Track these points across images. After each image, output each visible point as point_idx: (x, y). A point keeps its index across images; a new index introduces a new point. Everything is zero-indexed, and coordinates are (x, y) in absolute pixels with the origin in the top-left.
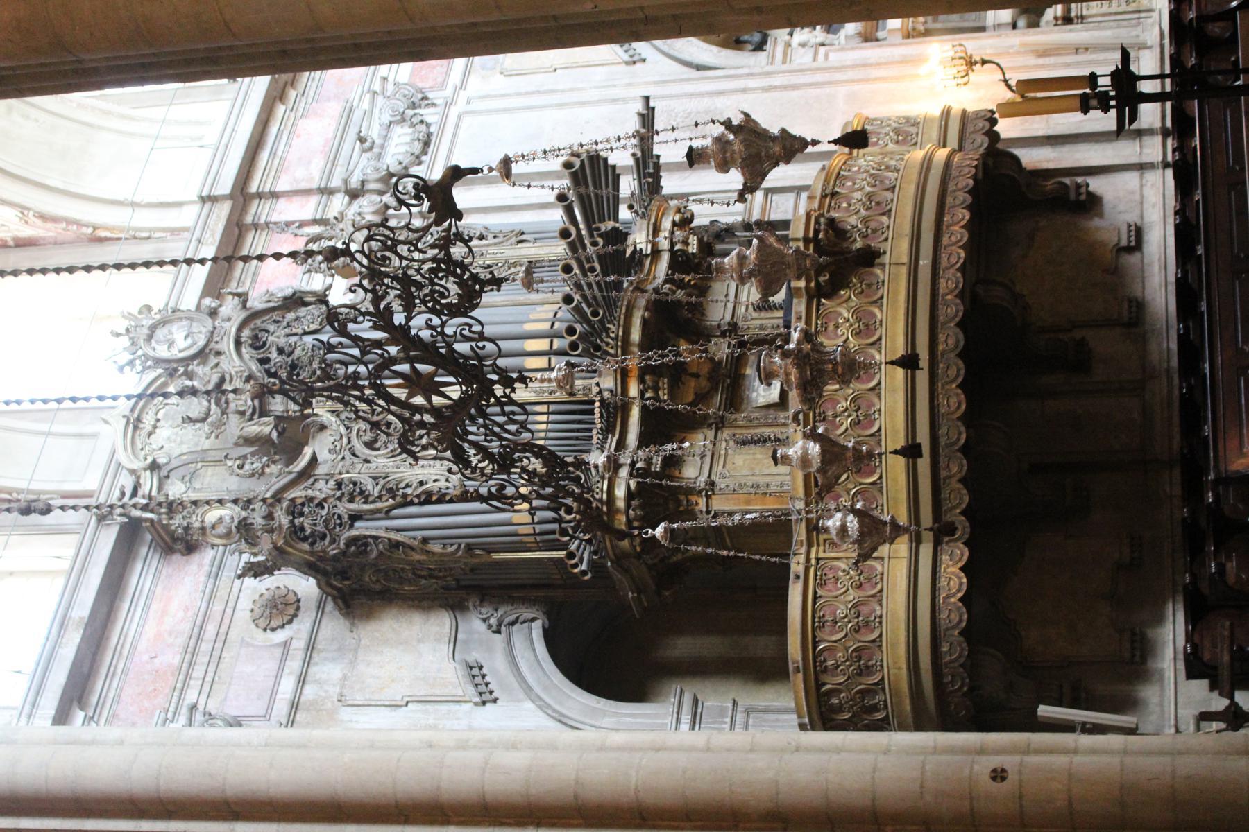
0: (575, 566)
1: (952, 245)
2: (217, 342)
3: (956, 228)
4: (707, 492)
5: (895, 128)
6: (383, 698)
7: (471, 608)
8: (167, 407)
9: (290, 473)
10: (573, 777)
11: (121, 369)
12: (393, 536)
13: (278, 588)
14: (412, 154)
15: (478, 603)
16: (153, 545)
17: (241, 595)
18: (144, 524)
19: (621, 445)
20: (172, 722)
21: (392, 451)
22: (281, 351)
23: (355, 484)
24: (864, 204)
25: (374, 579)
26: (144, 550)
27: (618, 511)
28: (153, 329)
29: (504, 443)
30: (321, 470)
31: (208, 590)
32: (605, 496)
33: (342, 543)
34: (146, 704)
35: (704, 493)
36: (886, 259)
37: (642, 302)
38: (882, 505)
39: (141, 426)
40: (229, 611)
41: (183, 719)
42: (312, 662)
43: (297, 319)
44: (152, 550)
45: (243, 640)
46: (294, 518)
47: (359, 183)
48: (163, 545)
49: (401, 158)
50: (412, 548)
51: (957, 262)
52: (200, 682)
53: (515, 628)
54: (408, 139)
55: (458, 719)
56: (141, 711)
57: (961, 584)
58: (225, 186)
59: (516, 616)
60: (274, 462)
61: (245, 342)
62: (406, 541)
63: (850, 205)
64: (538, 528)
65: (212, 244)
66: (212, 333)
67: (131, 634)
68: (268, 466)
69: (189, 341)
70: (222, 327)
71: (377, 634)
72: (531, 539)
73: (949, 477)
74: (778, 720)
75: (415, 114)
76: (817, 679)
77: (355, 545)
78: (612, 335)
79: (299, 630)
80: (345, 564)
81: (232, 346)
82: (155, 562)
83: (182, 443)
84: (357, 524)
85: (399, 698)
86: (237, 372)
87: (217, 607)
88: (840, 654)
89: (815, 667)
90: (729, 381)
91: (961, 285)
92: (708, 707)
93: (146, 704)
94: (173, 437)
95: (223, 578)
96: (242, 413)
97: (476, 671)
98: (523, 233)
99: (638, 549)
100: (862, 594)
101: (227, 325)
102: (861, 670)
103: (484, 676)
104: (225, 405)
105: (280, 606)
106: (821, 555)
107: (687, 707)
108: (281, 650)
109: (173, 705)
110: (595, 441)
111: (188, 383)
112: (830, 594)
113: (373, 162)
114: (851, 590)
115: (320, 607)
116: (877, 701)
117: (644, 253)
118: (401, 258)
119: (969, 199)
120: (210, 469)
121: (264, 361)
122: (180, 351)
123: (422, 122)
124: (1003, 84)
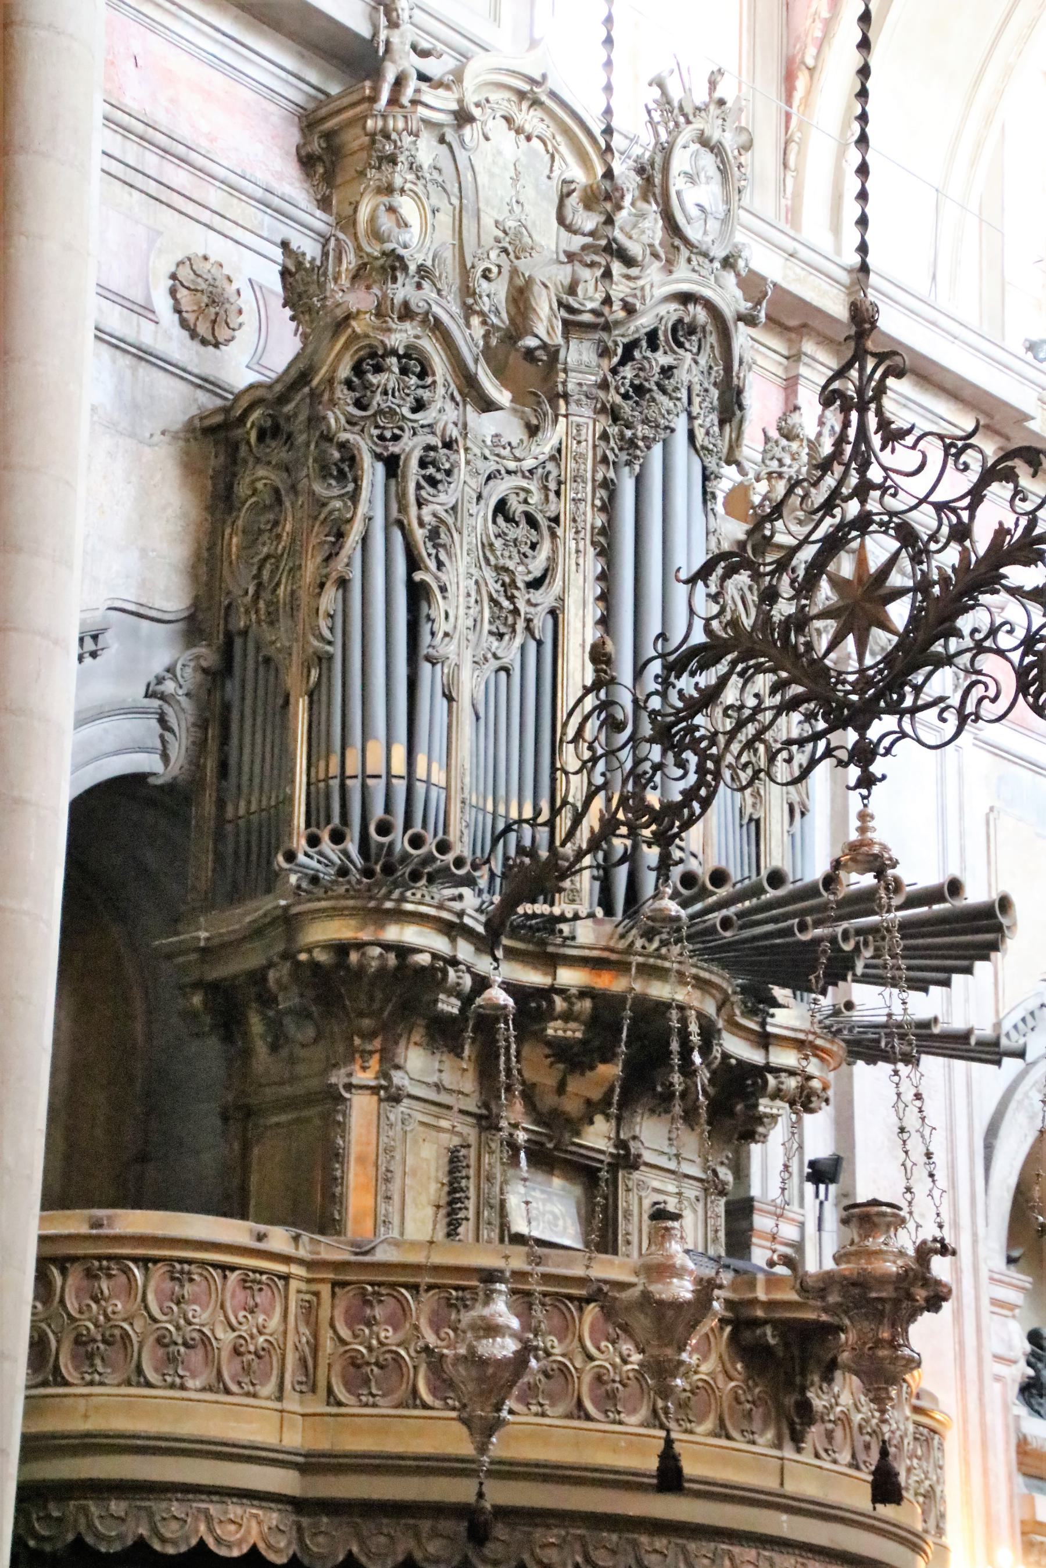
2: (689, 261)
4: (386, 1088)
8: (547, 157)
15: (204, 664)
17: (231, 242)
18: (368, 84)
21: (491, 545)
22: (667, 371)
23: (448, 473)
25: (259, 485)
26: (313, 77)
27: (382, 927)
28: (715, 149)
31: (243, 184)
32: (409, 907)
35: (383, 1082)
39: (525, 105)
40: (205, 216)
42: (118, 353)
44: (312, 91)
45: (160, 233)
46: (399, 357)
48: (323, 112)
53: (154, 723)
59: (176, 728)
60: (486, 336)
64: (354, 786)
66: (705, 255)
68: (484, 323)
69: (694, 212)
71: (158, 477)
72: (334, 769)
73: (417, 1536)
76: (74, 1259)
79: (170, 338)
80: (301, 438)
81: (685, 287)
83: (492, 175)
84: (380, 467)
86: (642, 288)
87: (214, 196)
88: (120, 1306)
89: (99, 1258)
90: (550, 1146)
95: (260, 214)
98: (803, 814)
99: (303, 957)
100: (225, 1355)
102: (85, 1344)
105: (213, 310)
106: (294, 1284)
112: (228, 1295)
115: (207, 384)
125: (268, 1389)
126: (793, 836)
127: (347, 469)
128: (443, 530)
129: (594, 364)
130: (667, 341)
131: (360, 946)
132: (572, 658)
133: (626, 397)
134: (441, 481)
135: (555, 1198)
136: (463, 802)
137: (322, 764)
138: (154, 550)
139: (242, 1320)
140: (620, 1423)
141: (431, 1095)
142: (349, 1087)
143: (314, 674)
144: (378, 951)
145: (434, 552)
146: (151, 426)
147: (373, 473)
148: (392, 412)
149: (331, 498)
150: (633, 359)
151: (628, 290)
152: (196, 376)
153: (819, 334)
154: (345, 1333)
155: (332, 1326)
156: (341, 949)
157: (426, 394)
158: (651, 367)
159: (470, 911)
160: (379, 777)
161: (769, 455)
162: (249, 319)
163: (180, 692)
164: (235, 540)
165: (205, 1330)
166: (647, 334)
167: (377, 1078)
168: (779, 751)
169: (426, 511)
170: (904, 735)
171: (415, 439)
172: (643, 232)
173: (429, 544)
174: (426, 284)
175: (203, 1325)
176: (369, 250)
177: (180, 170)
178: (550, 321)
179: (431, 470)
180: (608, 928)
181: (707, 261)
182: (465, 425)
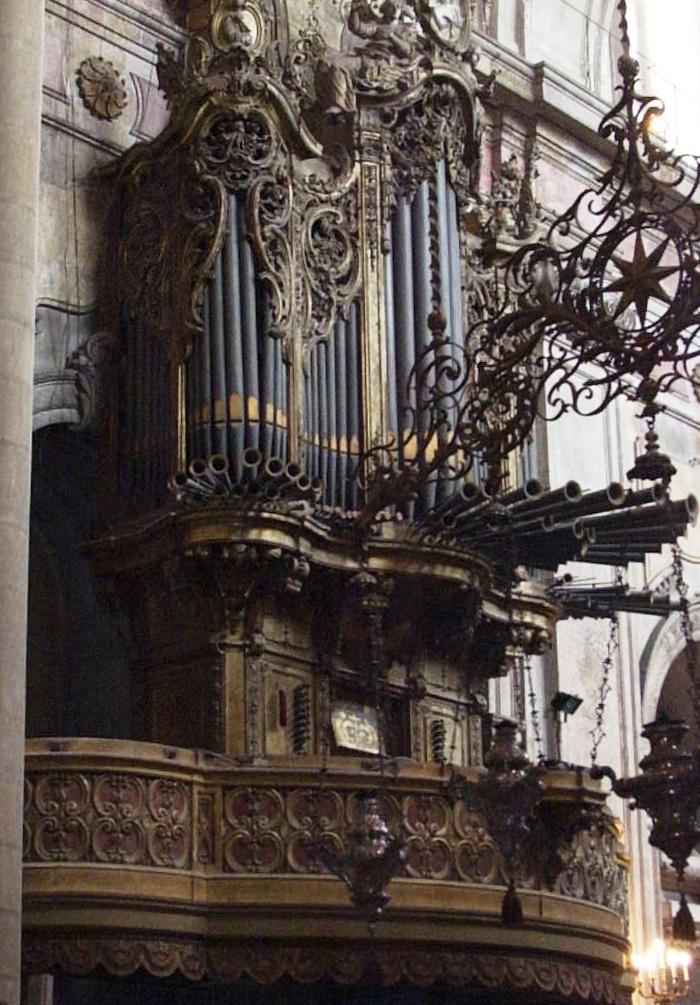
3: (574, 981)
4: (250, 646)
10: (7, 437)
12: (218, 241)
15: (106, 342)
17: (117, 49)
19: (317, 542)
21: (312, 253)
23: (281, 202)
30: (295, 161)
32: (266, 515)
33: (210, 177)
35: (248, 642)
36: (545, 892)
38: (256, 872)
40: (101, 31)
46: (245, 121)
53: (70, 387)
58: (552, 96)
59: (88, 389)
61: (441, 88)
66: (452, 50)
68: (299, 95)
69: (443, 22)
72: (206, 416)
77: (205, 194)
84: (233, 198)
86: (411, 73)
88: (75, 805)
96: (362, 72)
99: (190, 553)
102: (53, 832)
105: (106, 94)
106: (196, 789)
108: (57, 88)
110: (327, 508)
115: (104, 145)
121: (419, 107)
125: (180, 862)
128: (279, 242)
129: (379, 125)
131: (231, 545)
132: (371, 333)
133: (402, 148)
134: (276, 208)
141: (281, 651)
142: (224, 646)
143: (189, 348)
144: (243, 547)
145: (272, 258)
147: (228, 205)
148: (241, 160)
150: (406, 121)
151: (400, 74)
152: (97, 140)
154: (233, 821)
155: (224, 816)
156: (216, 547)
159: (308, 517)
160: (240, 421)
162: (131, 98)
163: (90, 364)
165: (137, 822)
166: (414, 104)
167: (242, 639)
168: (581, 390)
169: (266, 229)
170: (678, 376)
171: (258, 178)
172: (410, 35)
173: (270, 253)
174: (262, 71)
176: (220, 48)
178: (347, 96)
179: (269, 200)
180: (405, 527)
182: (291, 168)
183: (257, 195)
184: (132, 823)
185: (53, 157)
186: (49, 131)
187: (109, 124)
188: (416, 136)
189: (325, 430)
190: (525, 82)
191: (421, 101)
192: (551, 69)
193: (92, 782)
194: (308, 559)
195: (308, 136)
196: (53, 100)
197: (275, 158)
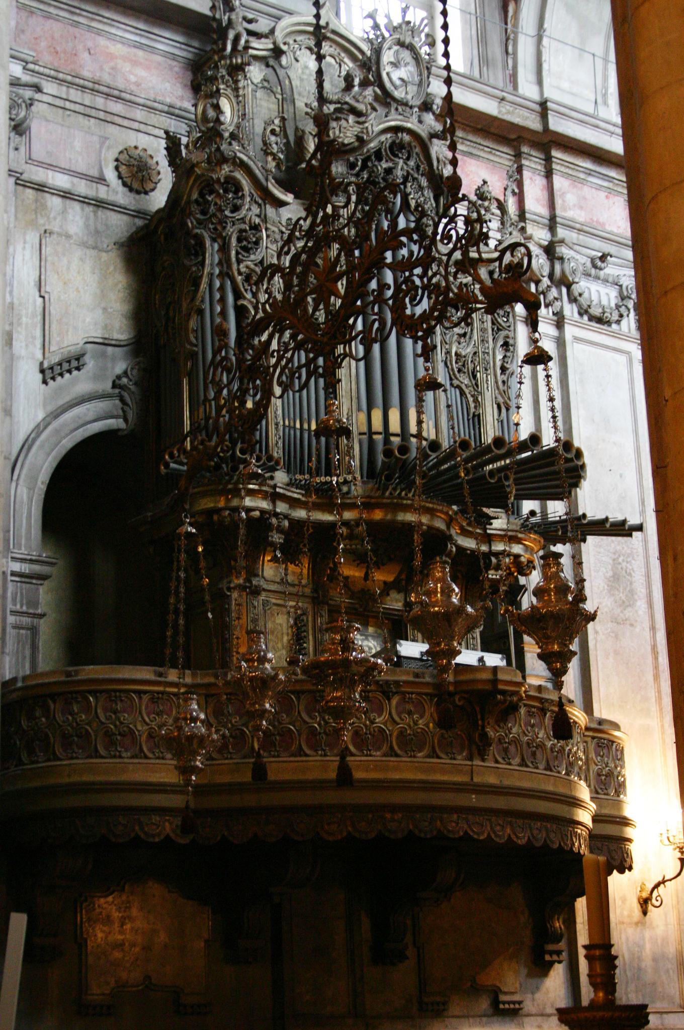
0: (172, 456)
1: (491, 827)
2: (397, 109)
3: (508, 831)
4: (250, 588)
5: (613, 773)
6: (48, 273)
7: (138, 360)
8: (337, 66)
9: (267, 180)
11: (371, 16)
12: (205, 280)
13: (159, 173)
14: (589, 306)
15: (142, 366)
16: (201, 53)
17: (152, 137)
19: (294, 503)
20: (24, 68)
23: (257, 243)
24: (533, 740)
26: (196, 44)
28: (411, 48)
29: (271, 369)
30: (270, 211)
31: (156, 105)
34: (43, 44)
37: (440, 524)
38: (231, 758)
40: (136, 125)
41: (26, 78)
42: (85, 205)
43: (421, 188)
44: (196, 51)
45: (107, 138)
47: (561, 255)
49: (586, 295)
50: (193, 299)
51: (473, 831)
52: (65, 97)
53: (117, 402)
54: (605, 302)
55: (27, 345)
56: (36, 39)
57: (153, 836)
58: (556, 124)
59: (130, 403)
60: (278, 166)
62: (200, 294)
63: (533, 726)
65: (500, 112)
66: (405, 104)
67: (113, 31)
68: (274, 159)
69: (398, 83)
70: (412, 114)
71: (112, 268)
72: (202, 415)
74: (24, 658)
75: (629, 310)
77: (196, 244)
78: (403, 493)
79: (117, 193)
81: (393, 123)
82: (184, 54)
83: (302, 80)
85: (48, 289)
86: (367, 128)
89: (71, 693)
91: (451, 836)
92: (38, 589)
93: (43, 44)
94: (307, 72)
95: (169, 120)
97: (74, 364)
101: (414, 119)
103: (69, 371)
104: (334, 117)
105: (140, 174)
107: (37, 568)
109: (41, 70)
110: (298, 477)
111: (357, 81)
113: (581, 268)
114: (146, 727)
115: (139, 213)
116: (39, 754)
117: (488, 527)
118: (450, 254)
119: (538, 844)
120: (275, 107)
121: (378, 155)
122: (388, 74)
123: (621, 316)
124: (660, 879)
126: (502, 421)
127: (198, 249)
129: (345, 172)
130: (387, 154)
131: (218, 511)
134: (251, 248)
135: (370, 638)
136: (277, 424)
137: (196, 413)
138: (111, 308)
139: (152, 719)
140: (371, 755)
142: (229, 589)
145: (249, 288)
146: (106, 242)
149: (191, 266)
151: (359, 130)
153: (529, 141)
157: (239, 202)
158: (378, 170)
159: (279, 485)
161: (471, 211)
163: (131, 383)
164: (157, 297)
165: (131, 726)
166: (374, 152)
169: (241, 266)
172: (365, 97)
173: (246, 284)
174: (233, 142)
175: (130, 724)
177: (118, 104)
179: (245, 243)
181: (408, 109)
183: (234, 242)
184: (128, 727)
185: (96, 228)
186: (89, 209)
187: (147, 197)
188: (376, 177)
189: (305, 416)
190: (534, 116)
191: (380, 149)
192: (553, 103)
193: (96, 698)
194: (286, 517)
195: (277, 189)
196: (94, 184)
197: (250, 209)
